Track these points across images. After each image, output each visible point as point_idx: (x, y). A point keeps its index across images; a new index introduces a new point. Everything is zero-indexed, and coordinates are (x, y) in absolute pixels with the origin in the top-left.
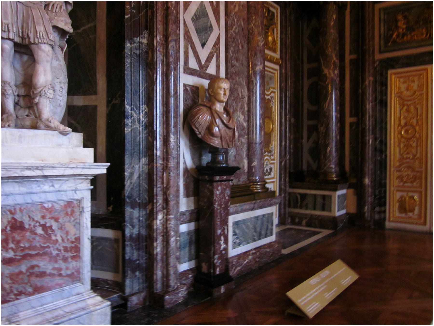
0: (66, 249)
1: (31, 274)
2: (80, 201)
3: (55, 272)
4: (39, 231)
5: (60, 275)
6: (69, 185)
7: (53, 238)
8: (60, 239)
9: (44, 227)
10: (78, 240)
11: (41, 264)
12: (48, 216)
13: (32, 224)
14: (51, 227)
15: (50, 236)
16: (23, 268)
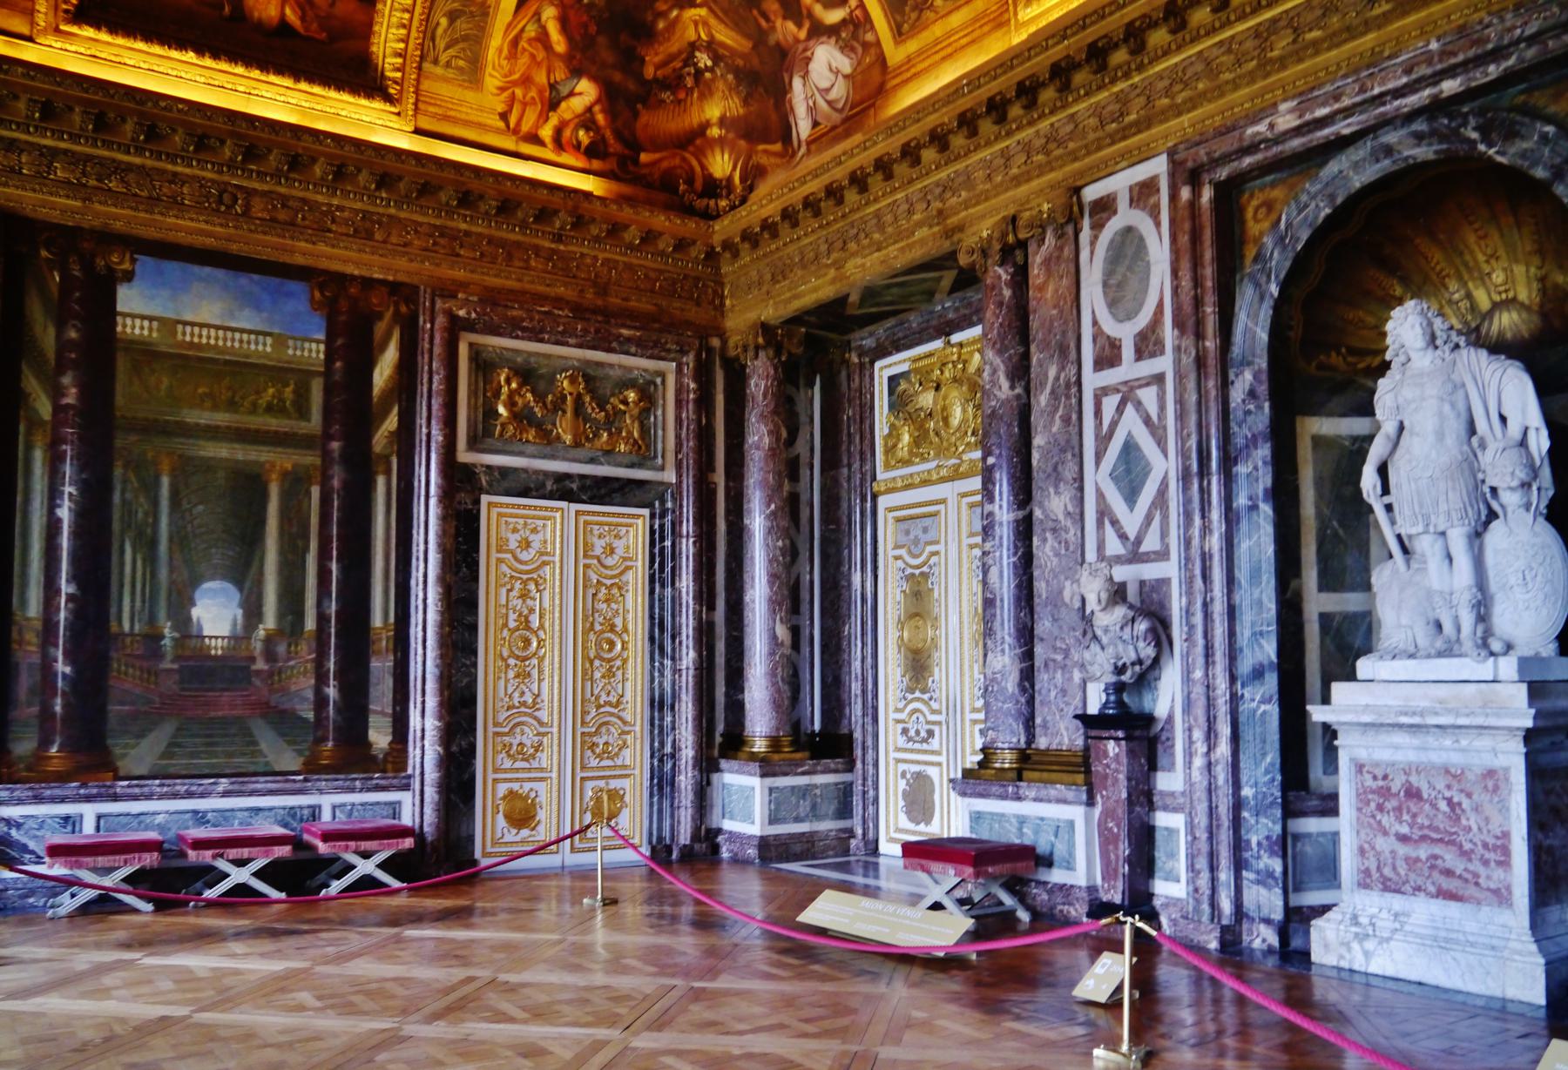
0: (1485, 845)
1: (1432, 867)
2: (1507, 770)
3: (1469, 876)
4: (1443, 806)
5: (1477, 884)
6: (1484, 742)
7: (1464, 822)
8: (1475, 828)
9: (1450, 801)
10: (1506, 835)
11: (1448, 857)
12: (1456, 786)
13: (1434, 794)
14: (1460, 804)
15: (1459, 819)
16: (1423, 856)
